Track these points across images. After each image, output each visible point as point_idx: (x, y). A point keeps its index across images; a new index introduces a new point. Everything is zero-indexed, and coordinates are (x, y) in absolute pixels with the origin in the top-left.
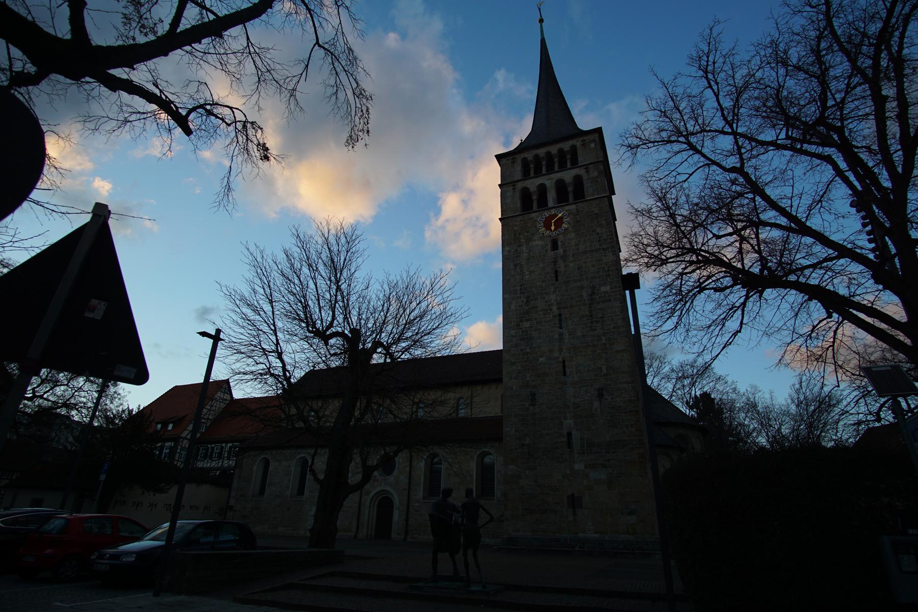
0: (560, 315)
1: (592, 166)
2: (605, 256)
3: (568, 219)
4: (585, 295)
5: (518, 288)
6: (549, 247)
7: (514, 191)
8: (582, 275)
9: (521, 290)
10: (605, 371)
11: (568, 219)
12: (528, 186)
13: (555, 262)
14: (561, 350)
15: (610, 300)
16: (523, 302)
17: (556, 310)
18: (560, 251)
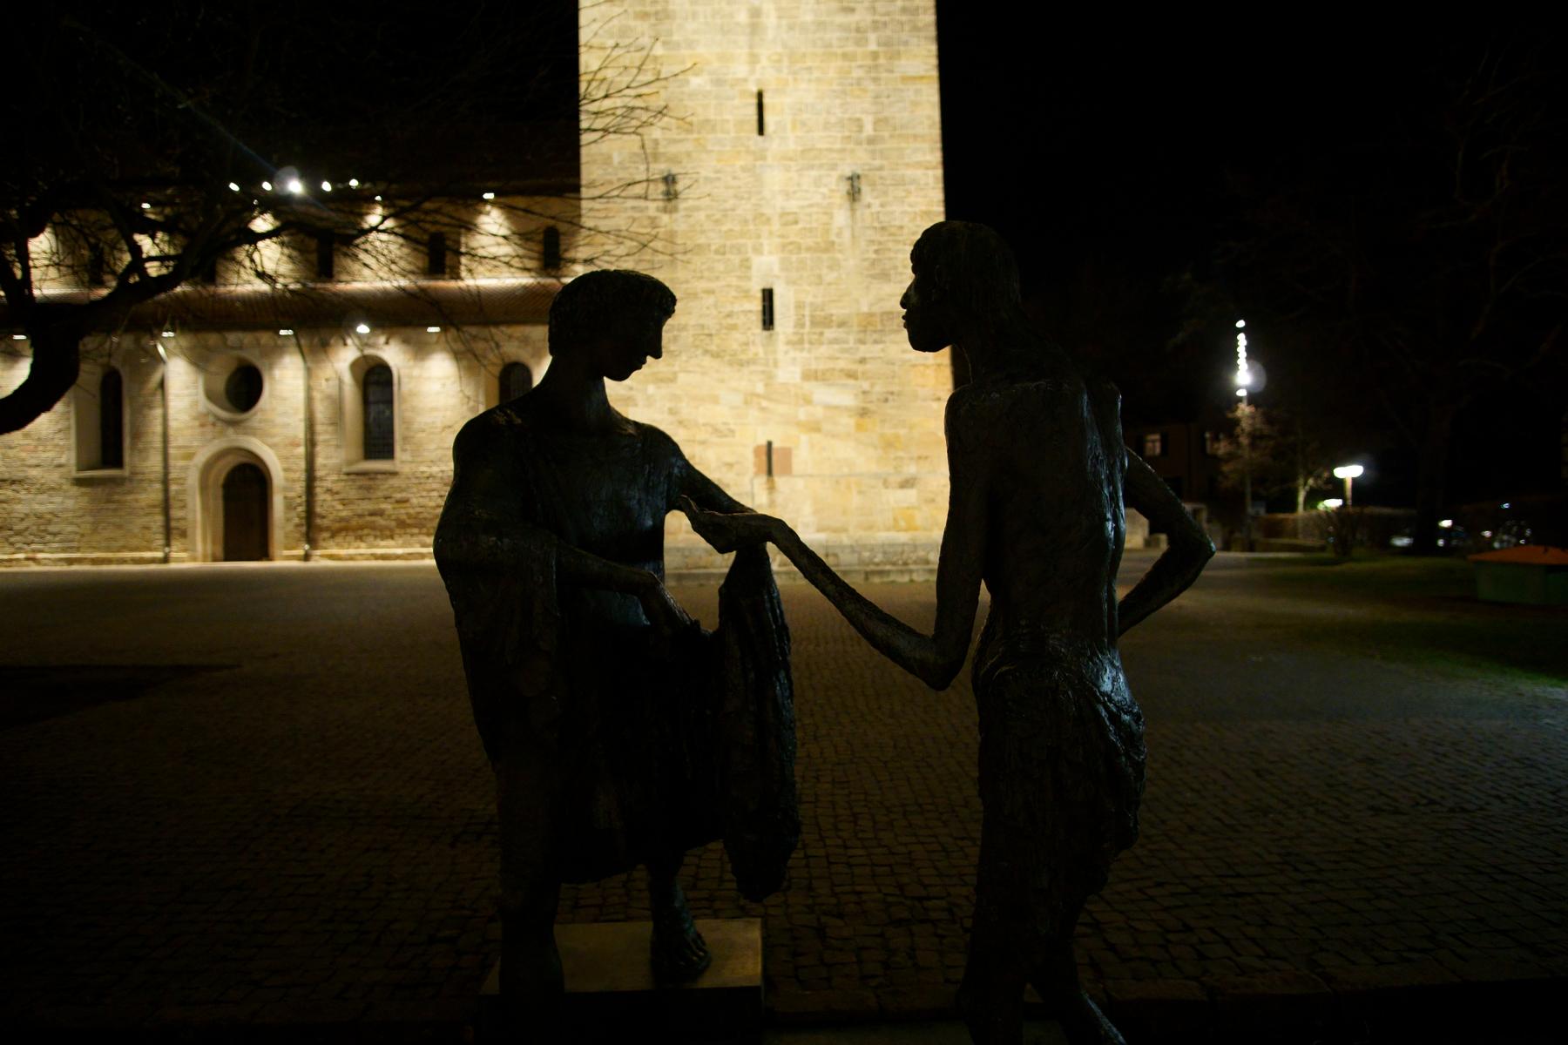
10: (869, 130)
14: (754, 59)
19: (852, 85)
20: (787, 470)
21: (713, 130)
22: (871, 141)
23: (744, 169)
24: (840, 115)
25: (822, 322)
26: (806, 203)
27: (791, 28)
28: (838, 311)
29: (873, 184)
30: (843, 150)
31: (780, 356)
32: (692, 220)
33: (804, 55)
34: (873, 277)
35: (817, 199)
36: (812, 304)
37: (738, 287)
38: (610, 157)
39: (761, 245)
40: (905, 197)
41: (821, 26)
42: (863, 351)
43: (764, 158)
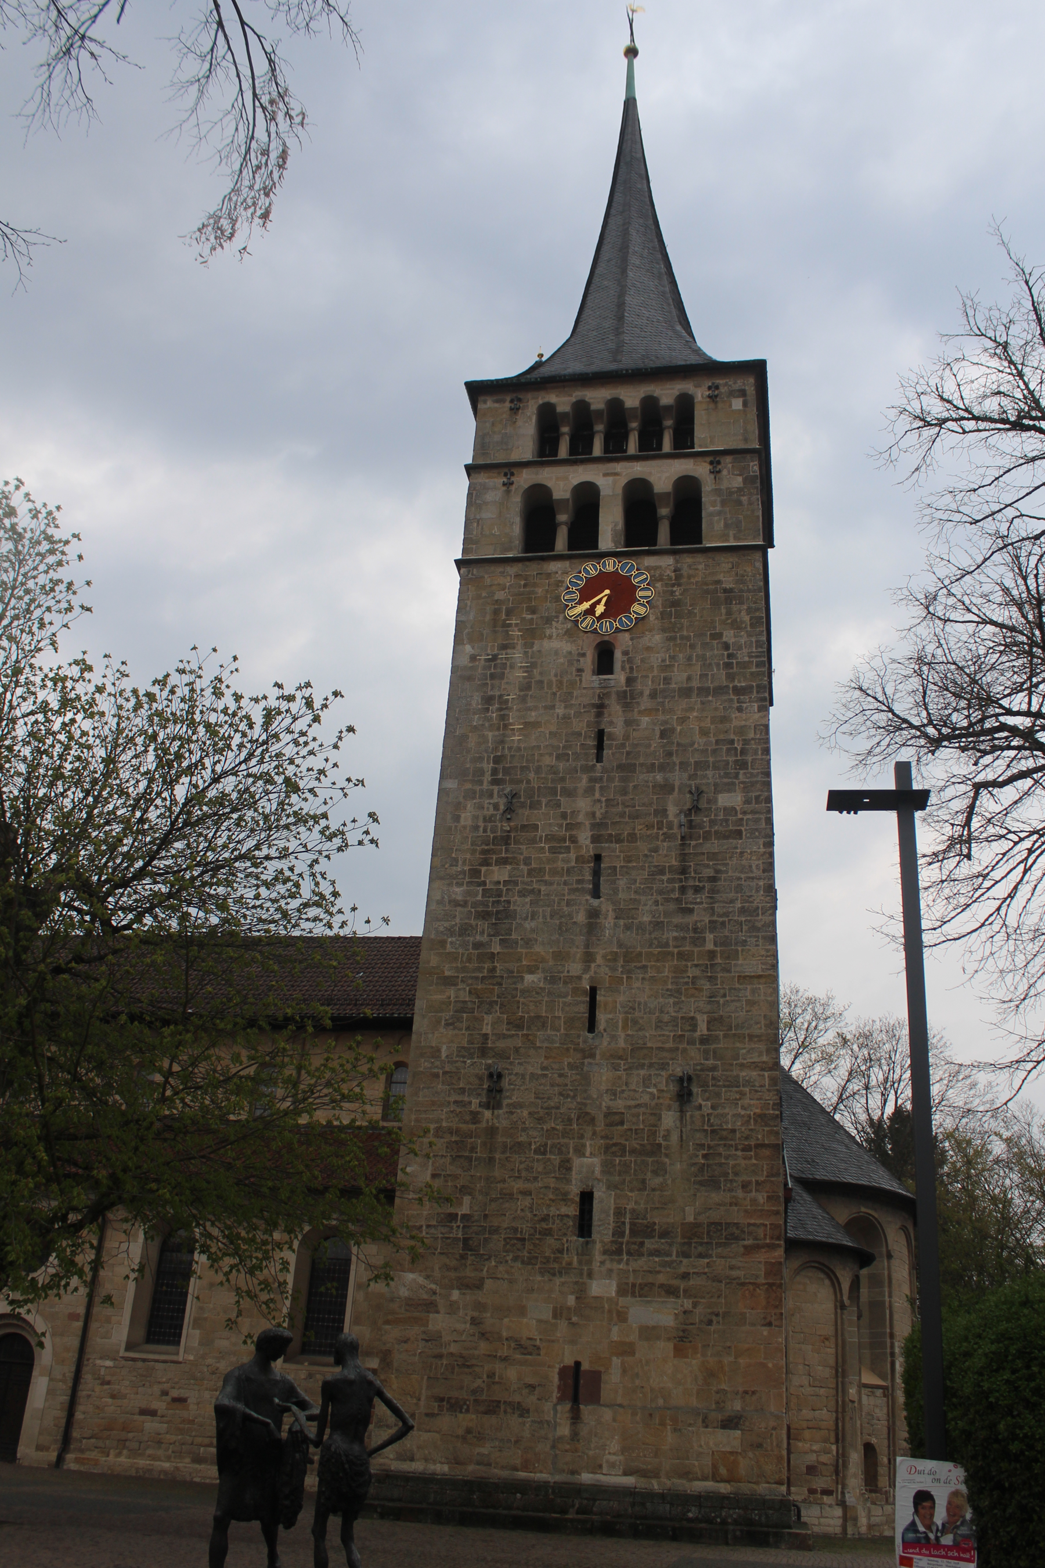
0: (598, 858)
1: (728, 459)
2: (740, 710)
3: (649, 593)
4: (672, 810)
5: (488, 766)
6: (589, 662)
7: (508, 492)
8: (670, 754)
9: (495, 772)
10: (702, 1028)
11: (649, 593)
12: (549, 484)
13: (600, 708)
14: (589, 958)
15: (739, 834)
16: (496, 807)
17: (588, 842)
18: (619, 677)
19: (687, 983)
20: (595, 1398)
21: (544, 1025)
22: (704, 1040)
23: (571, 1066)
24: (673, 1014)
25: (643, 1230)
26: (633, 1103)
27: (628, 928)
28: (659, 1219)
29: (704, 1085)
30: (671, 1050)
31: (595, 1266)
32: (514, 1117)
33: (640, 954)
34: (701, 1183)
35: (646, 1098)
36: (633, 1211)
37: (557, 1189)
38: (439, 1050)
39: (584, 1146)
40: (740, 1099)
41: (658, 925)
42: (685, 1266)
43: (592, 1056)
